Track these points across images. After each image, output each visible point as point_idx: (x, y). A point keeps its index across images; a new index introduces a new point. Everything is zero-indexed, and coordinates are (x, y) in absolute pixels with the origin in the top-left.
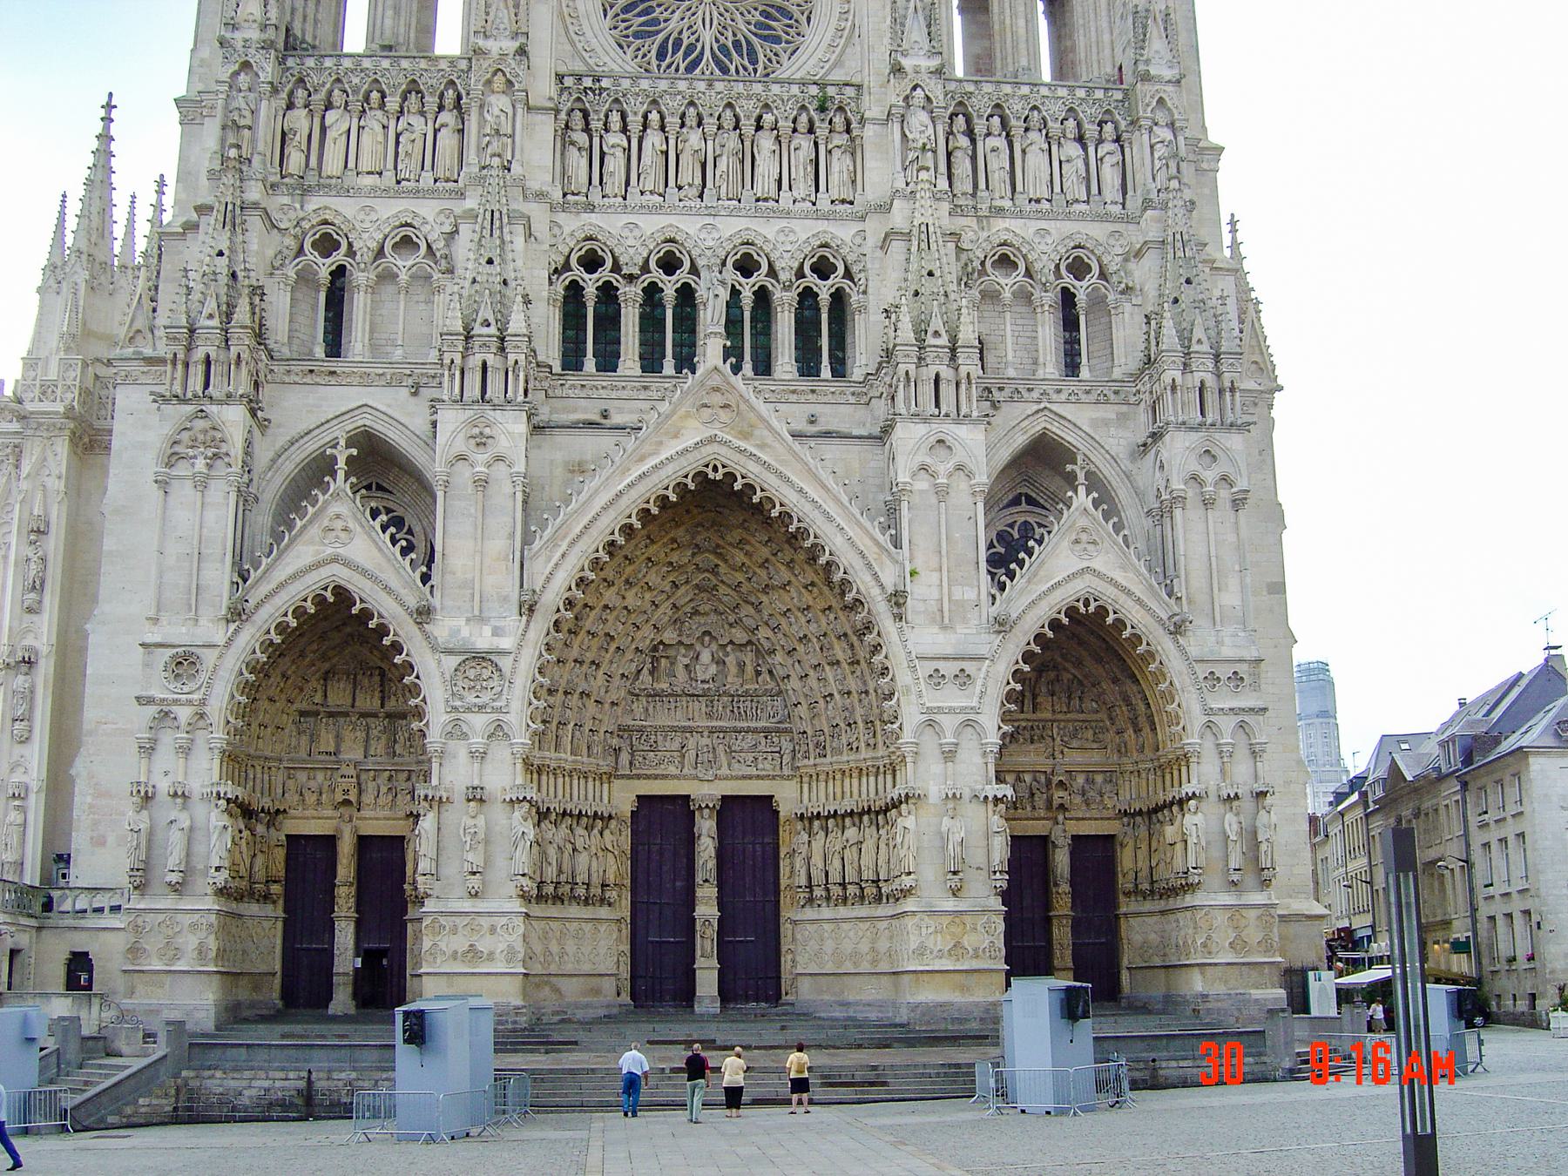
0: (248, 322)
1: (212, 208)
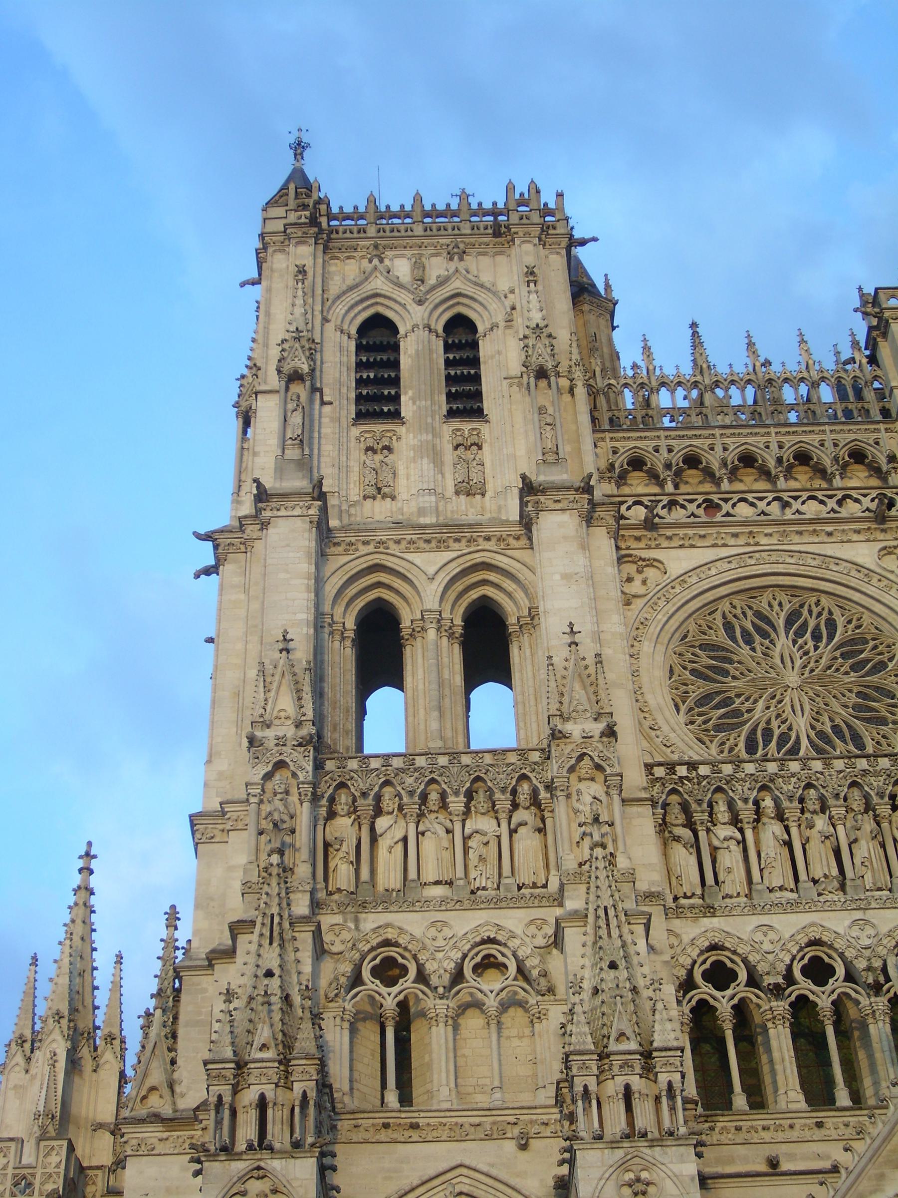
0: (313, 1050)
1: (253, 923)
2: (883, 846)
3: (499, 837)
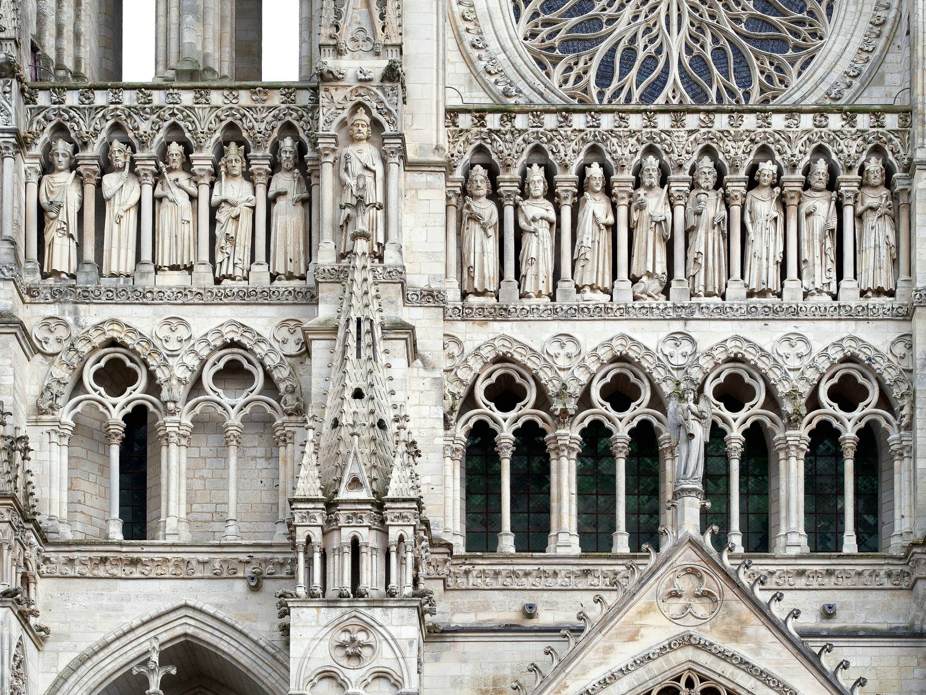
2: (727, 237)
3: (254, 208)
